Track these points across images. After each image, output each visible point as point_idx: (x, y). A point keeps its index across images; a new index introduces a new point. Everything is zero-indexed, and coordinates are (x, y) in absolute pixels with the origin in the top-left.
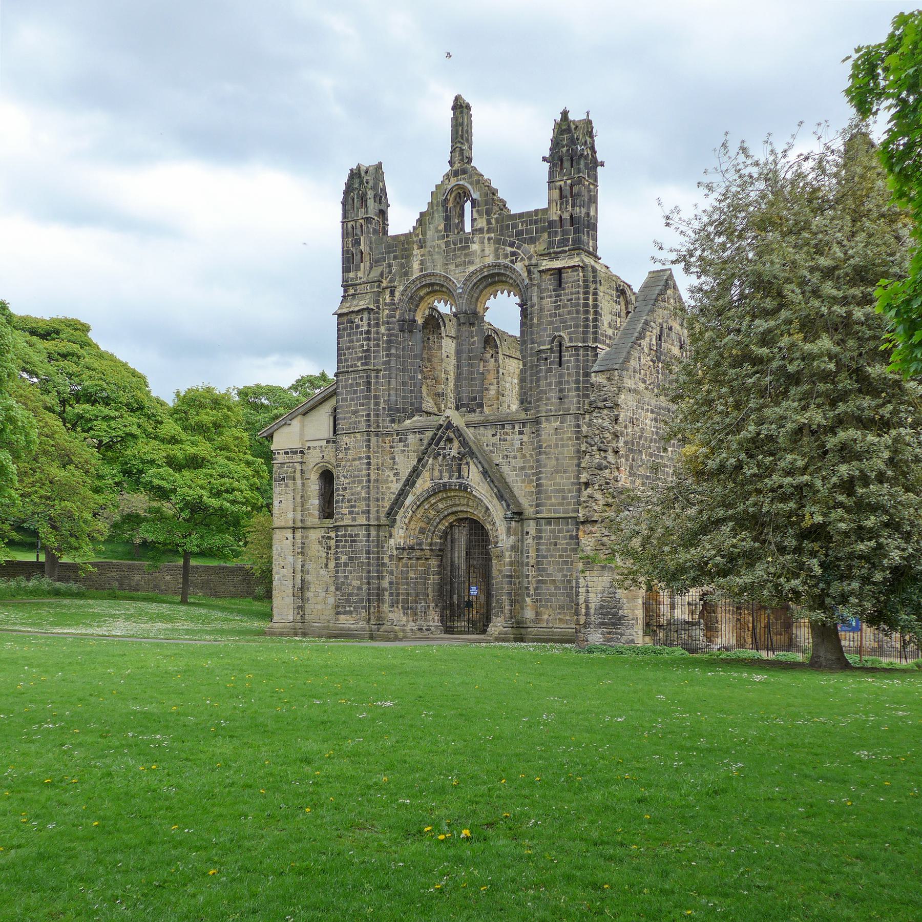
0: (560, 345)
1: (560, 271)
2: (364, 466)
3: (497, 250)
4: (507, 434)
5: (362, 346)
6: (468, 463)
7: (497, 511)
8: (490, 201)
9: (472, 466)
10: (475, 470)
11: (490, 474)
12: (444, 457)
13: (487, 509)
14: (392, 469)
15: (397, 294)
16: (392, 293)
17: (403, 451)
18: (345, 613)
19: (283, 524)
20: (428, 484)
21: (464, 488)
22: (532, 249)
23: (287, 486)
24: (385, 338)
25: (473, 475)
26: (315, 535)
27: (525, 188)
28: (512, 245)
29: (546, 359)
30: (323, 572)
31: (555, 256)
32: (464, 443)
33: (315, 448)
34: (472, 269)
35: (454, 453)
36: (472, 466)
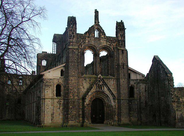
0: (123, 65)
1: (123, 50)
2: (77, 85)
3: (106, 43)
4: (110, 81)
5: (76, 57)
6: (104, 87)
7: (111, 97)
8: (101, 32)
9: (105, 87)
10: (106, 88)
11: (109, 89)
12: (98, 85)
13: (108, 96)
14: (82, 86)
15: (82, 47)
16: (81, 46)
17: (85, 82)
18: (71, 120)
19: (48, 98)
20: (94, 90)
21: (103, 92)
22: (114, 44)
23: (49, 87)
24: (80, 56)
25: (105, 89)
26: (56, 101)
27: (111, 32)
28: (110, 42)
29: (121, 67)
30: (58, 110)
31: (121, 47)
32: (104, 82)
33: (56, 79)
34: (101, 45)
35: (101, 84)
36: (105, 87)
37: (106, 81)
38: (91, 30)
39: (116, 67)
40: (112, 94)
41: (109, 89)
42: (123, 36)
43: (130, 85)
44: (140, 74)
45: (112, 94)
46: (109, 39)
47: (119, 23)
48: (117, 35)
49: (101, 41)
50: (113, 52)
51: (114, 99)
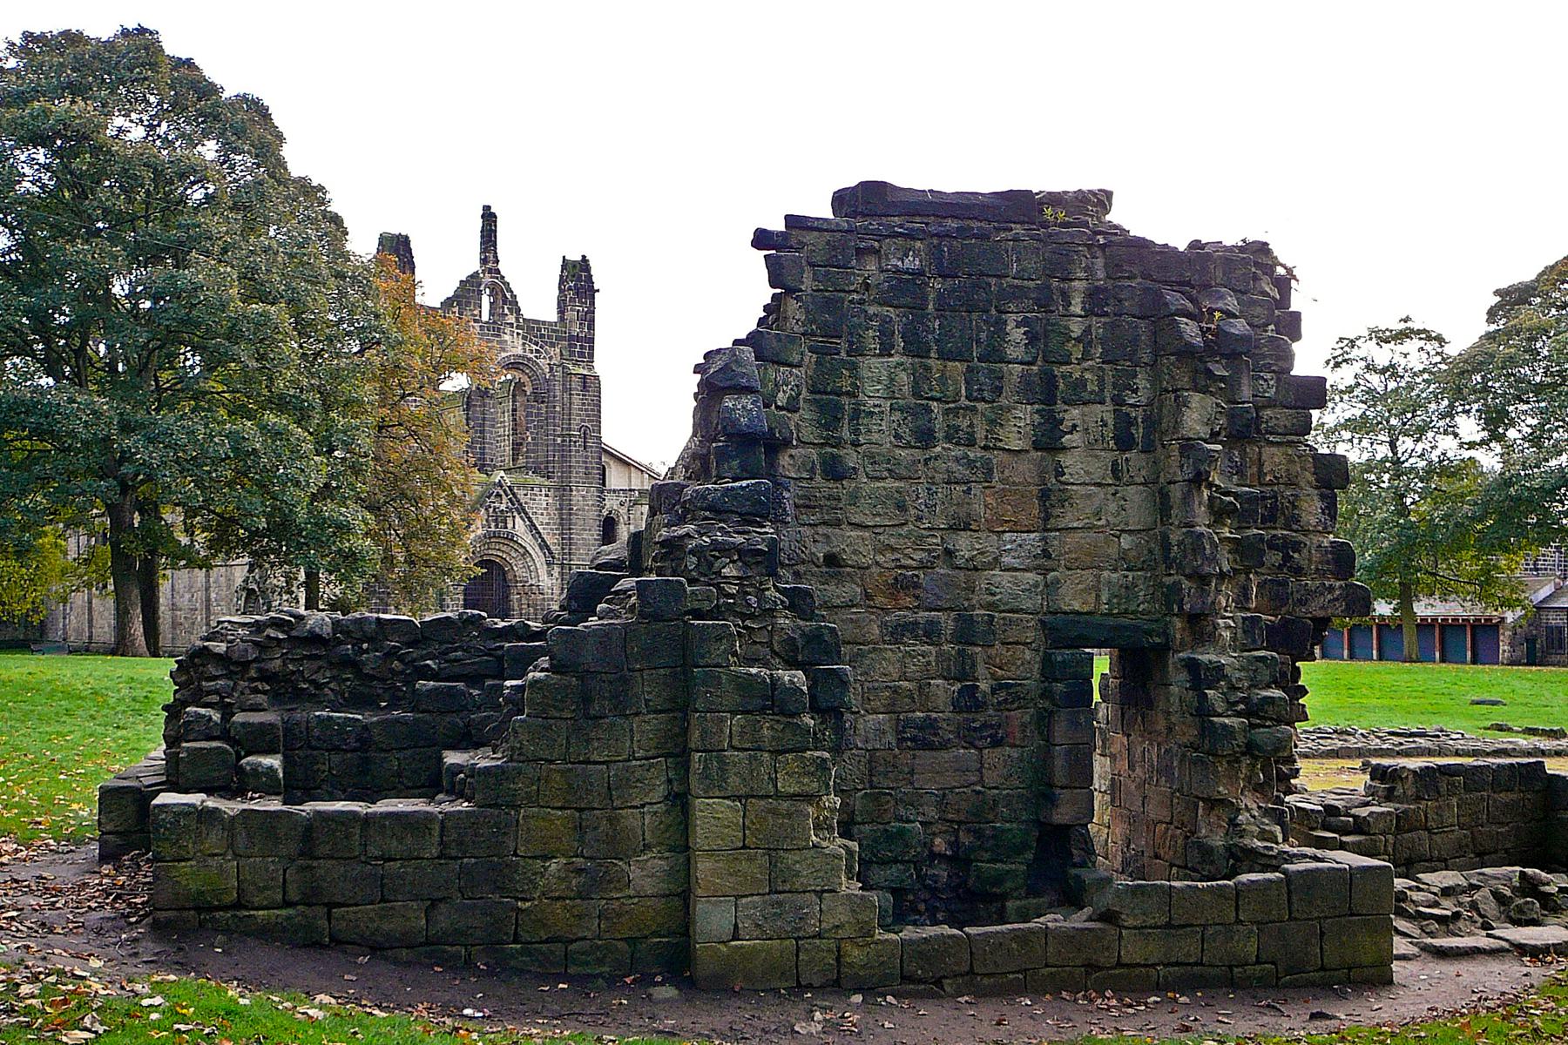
8: (505, 298)
9: (518, 519)
11: (532, 526)
20: (479, 532)
25: (520, 527)
27: (539, 299)
32: (514, 500)
36: (518, 519)
37: (520, 493)
38: (468, 291)
39: (559, 440)
40: (544, 546)
41: (532, 526)
42: (589, 319)
43: (605, 512)
44: (640, 468)
45: (544, 546)
46: (532, 329)
47: (574, 264)
48: (561, 311)
49: (507, 337)
50: (547, 381)
51: (548, 564)
